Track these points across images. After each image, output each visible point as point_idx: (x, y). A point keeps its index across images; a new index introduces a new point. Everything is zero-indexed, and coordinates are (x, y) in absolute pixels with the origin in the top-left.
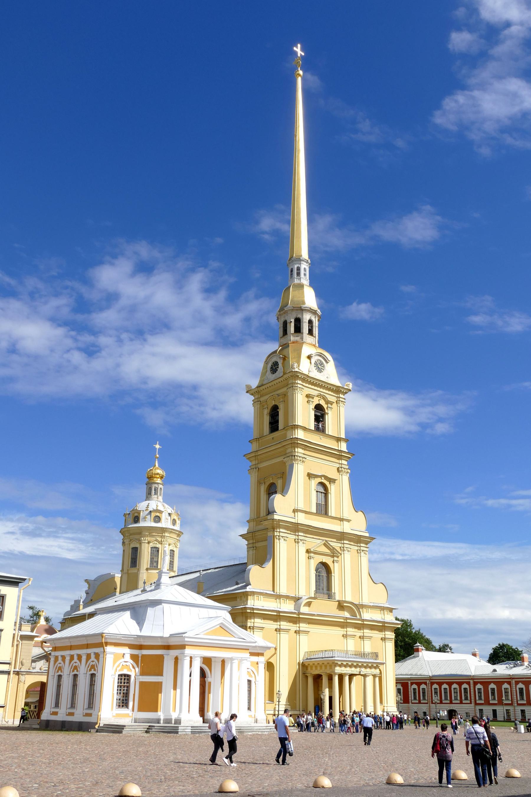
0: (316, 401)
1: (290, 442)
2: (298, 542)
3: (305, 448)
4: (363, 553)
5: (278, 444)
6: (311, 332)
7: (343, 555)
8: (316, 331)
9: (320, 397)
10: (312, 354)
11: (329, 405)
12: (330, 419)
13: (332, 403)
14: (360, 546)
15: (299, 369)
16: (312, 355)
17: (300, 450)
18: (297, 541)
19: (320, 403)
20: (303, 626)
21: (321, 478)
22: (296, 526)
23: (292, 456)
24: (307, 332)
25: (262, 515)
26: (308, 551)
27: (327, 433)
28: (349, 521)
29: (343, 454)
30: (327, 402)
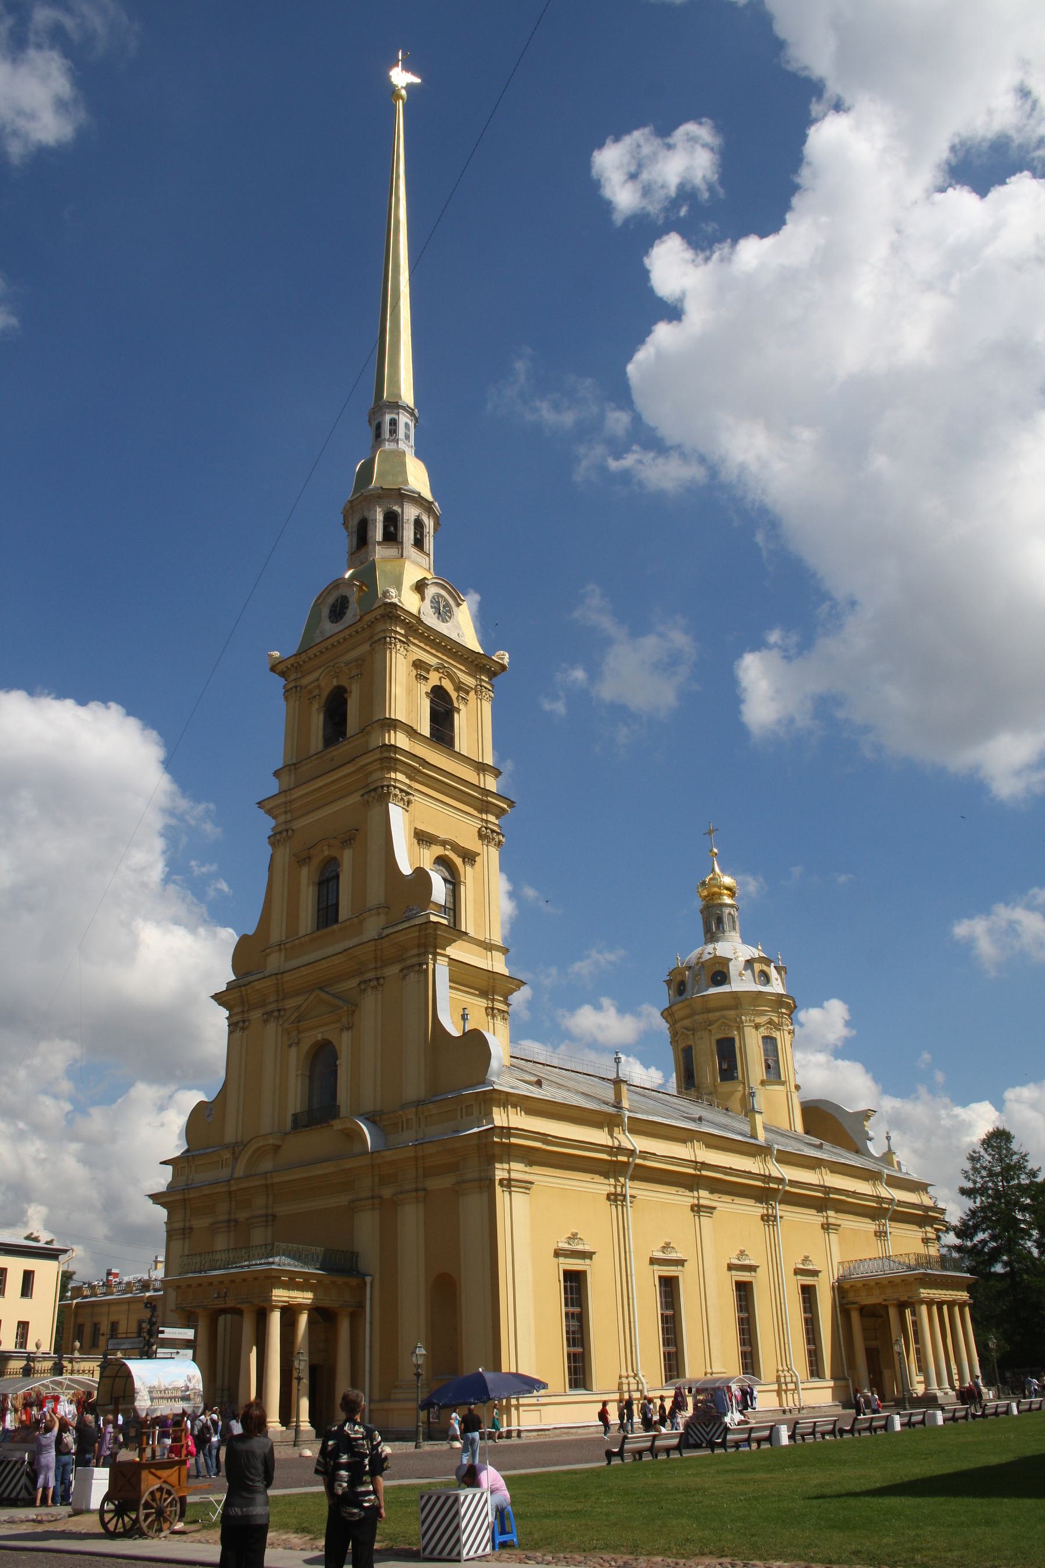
0: (434, 679)
1: (378, 756)
3: (413, 774)
5: (350, 765)
6: (419, 544)
8: (429, 543)
9: (443, 673)
10: (428, 579)
11: (462, 695)
12: (461, 721)
15: (400, 601)
16: (426, 581)
17: (400, 777)
23: (382, 787)
24: (412, 543)
25: (302, 932)
30: (459, 687)
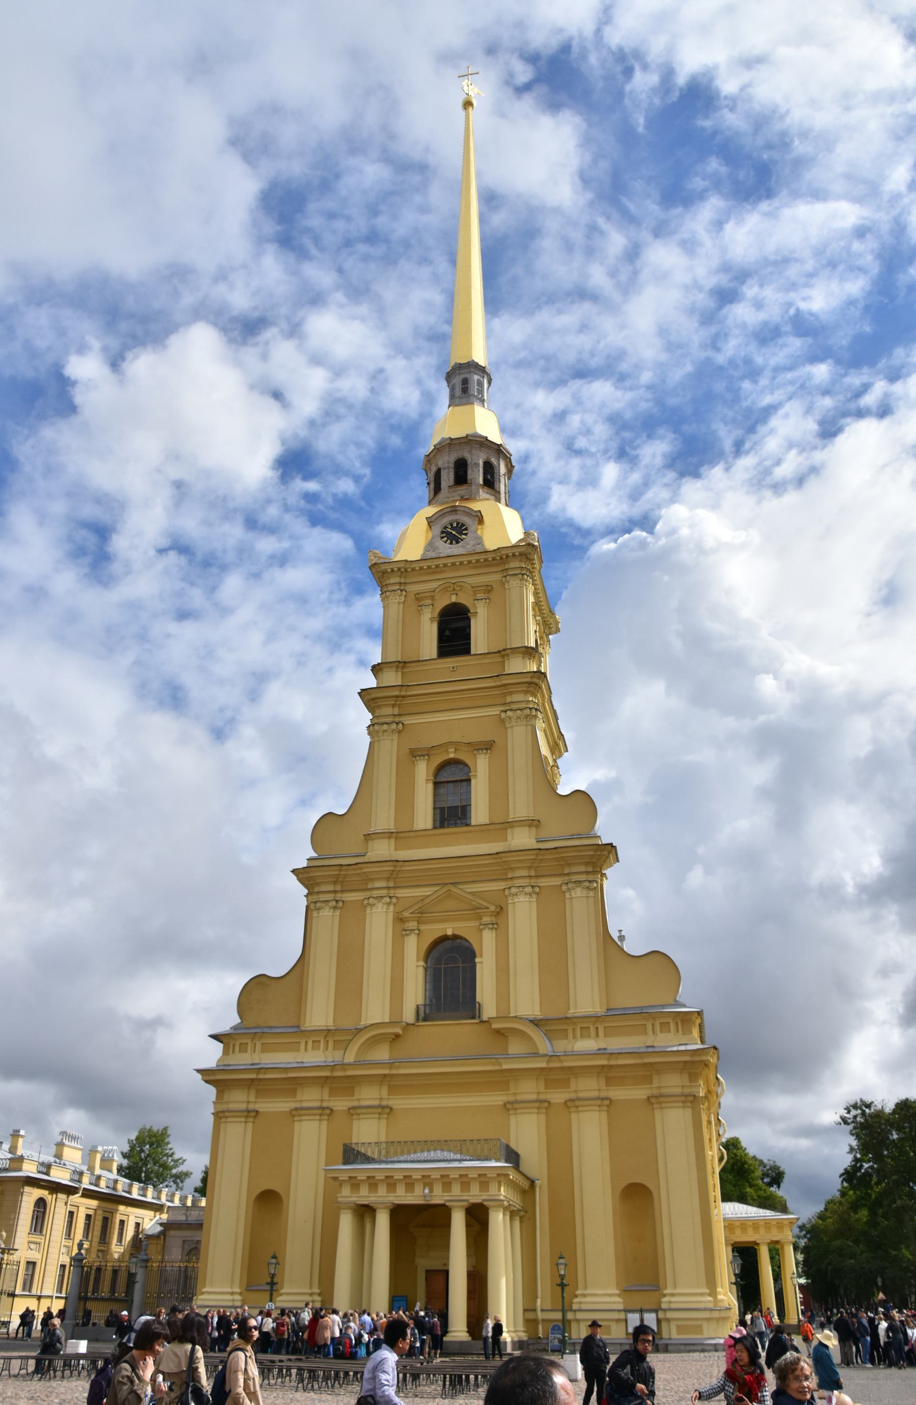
2: (372, 905)
4: (579, 890)
7: (510, 906)
11: (479, 596)
13: (489, 589)
14: (568, 874)
18: (363, 906)
19: (454, 599)
20: (369, 1095)
21: (447, 750)
22: (358, 872)
26: (400, 920)
27: (472, 653)
28: (533, 823)
29: (504, 682)
30: (475, 589)
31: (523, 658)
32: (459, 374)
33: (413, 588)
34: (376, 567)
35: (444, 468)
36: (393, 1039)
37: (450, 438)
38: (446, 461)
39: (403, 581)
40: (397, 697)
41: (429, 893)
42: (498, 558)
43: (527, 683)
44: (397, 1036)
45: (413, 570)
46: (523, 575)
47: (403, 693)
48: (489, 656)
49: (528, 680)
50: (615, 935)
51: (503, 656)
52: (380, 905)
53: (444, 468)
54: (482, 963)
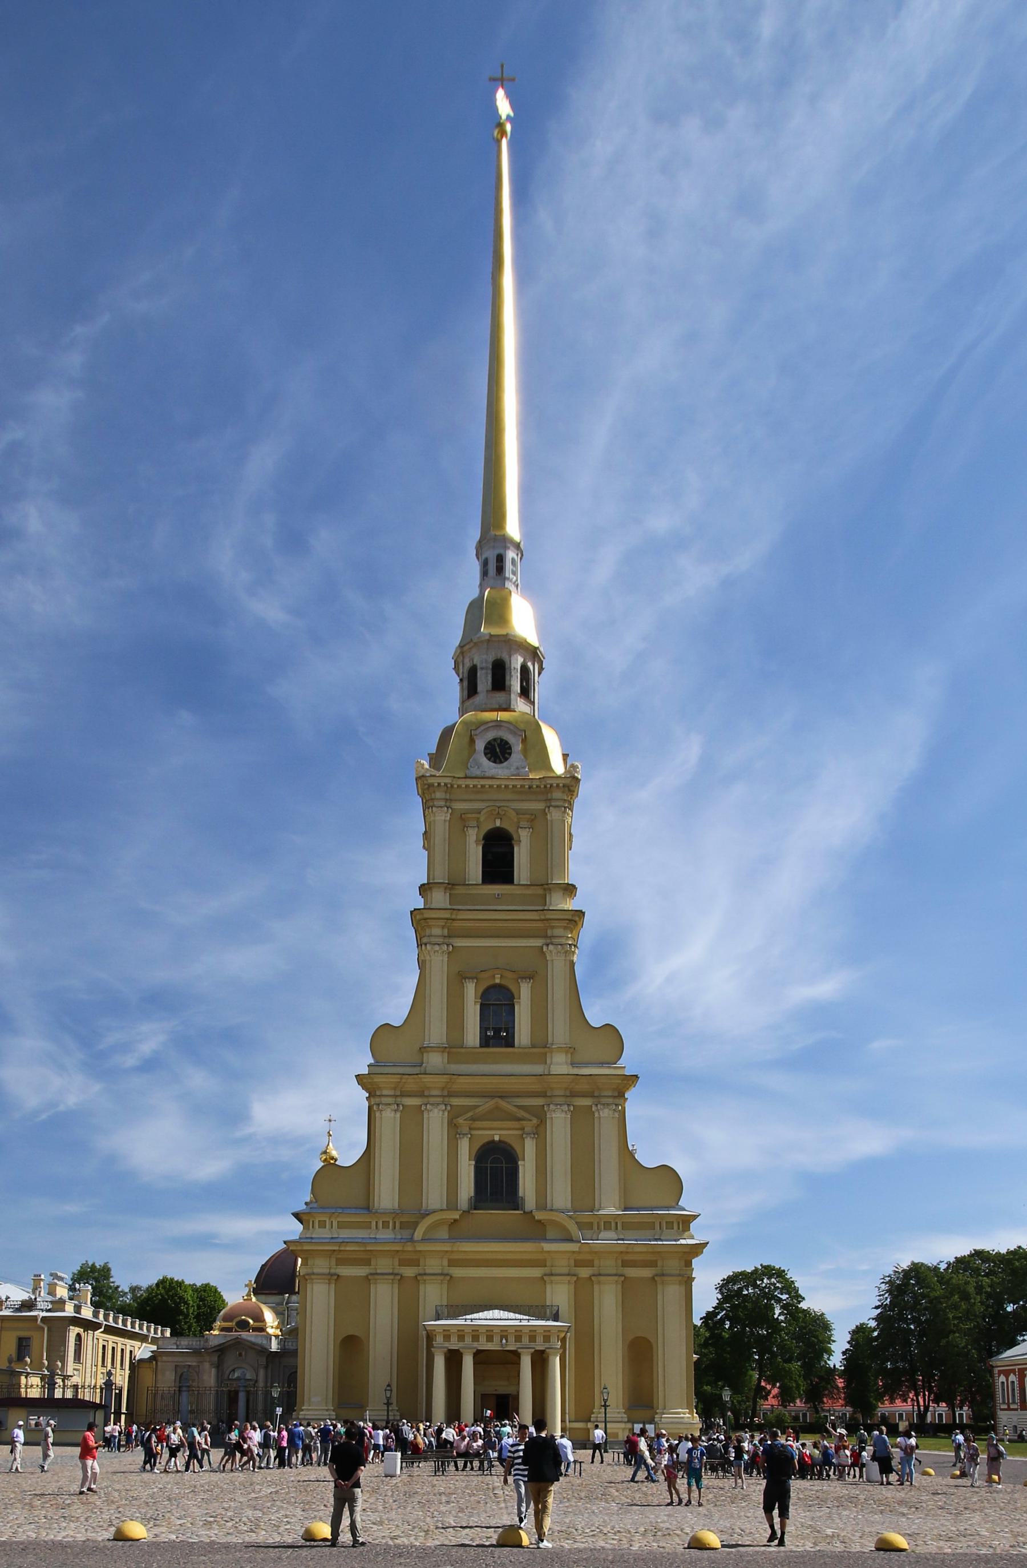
19: (498, 824)
26: (452, 1125)
29: (548, 917)
31: (564, 894)
32: (494, 547)
33: (459, 806)
34: (423, 779)
35: (482, 669)
36: (452, 1223)
37: (490, 634)
38: (483, 660)
39: (448, 797)
40: (447, 919)
41: (481, 1104)
42: (542, 786)
43: (567, 920)
44: (455, 1220)
45: (459, 786)
46: (565, 808)
47: (454, 917)
48: (532, 887)
49: (570, 917)
50: (631, 1148)
51: (545, 889)
52: (436, 1111)
53: (482, 669)
54: (524, 1165)
